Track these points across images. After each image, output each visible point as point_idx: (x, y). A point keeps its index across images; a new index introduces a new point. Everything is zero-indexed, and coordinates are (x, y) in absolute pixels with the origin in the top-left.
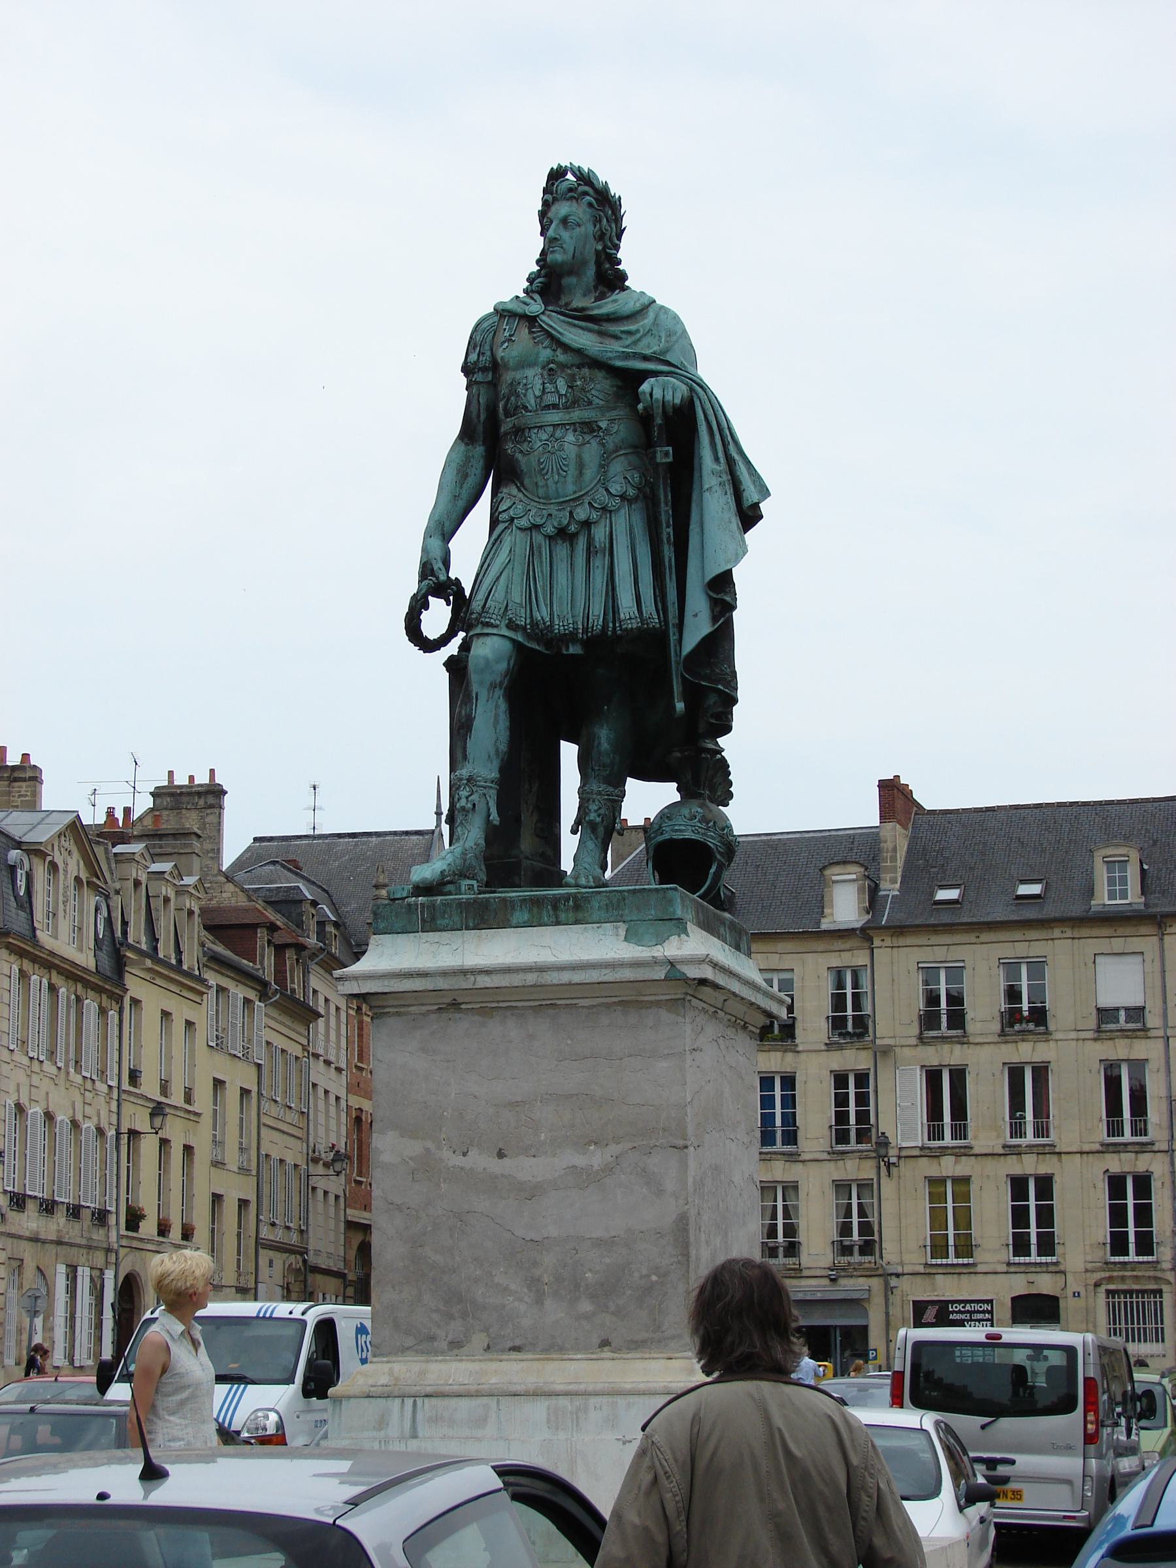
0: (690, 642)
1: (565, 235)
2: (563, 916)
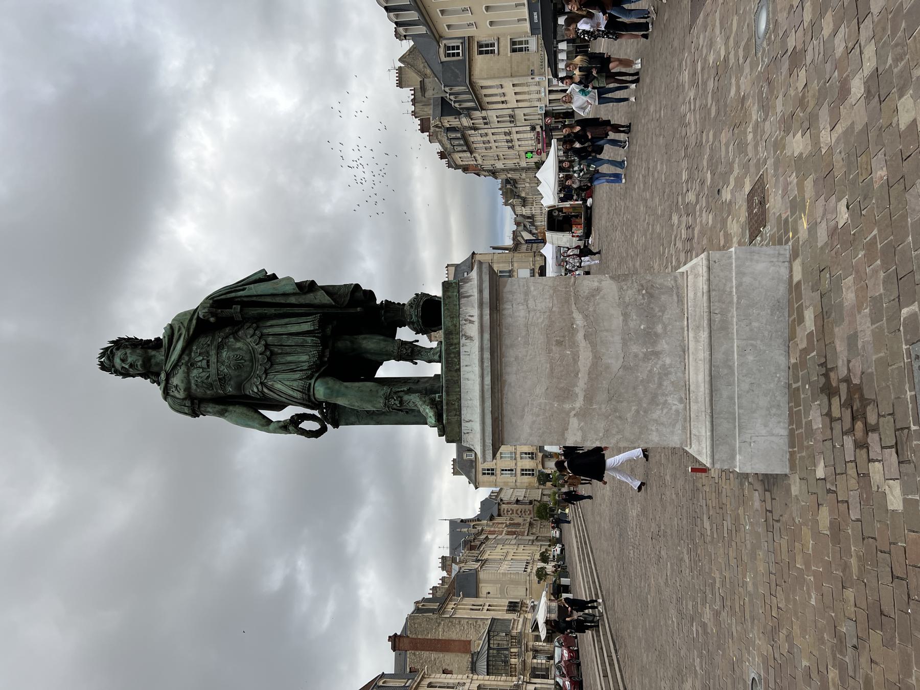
0: (327, 300)
1: (130, 360)
2: (455, 341)
